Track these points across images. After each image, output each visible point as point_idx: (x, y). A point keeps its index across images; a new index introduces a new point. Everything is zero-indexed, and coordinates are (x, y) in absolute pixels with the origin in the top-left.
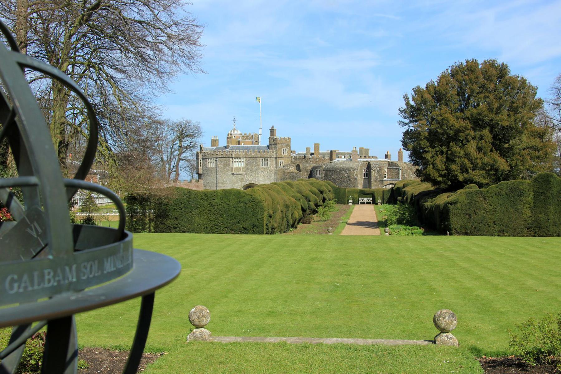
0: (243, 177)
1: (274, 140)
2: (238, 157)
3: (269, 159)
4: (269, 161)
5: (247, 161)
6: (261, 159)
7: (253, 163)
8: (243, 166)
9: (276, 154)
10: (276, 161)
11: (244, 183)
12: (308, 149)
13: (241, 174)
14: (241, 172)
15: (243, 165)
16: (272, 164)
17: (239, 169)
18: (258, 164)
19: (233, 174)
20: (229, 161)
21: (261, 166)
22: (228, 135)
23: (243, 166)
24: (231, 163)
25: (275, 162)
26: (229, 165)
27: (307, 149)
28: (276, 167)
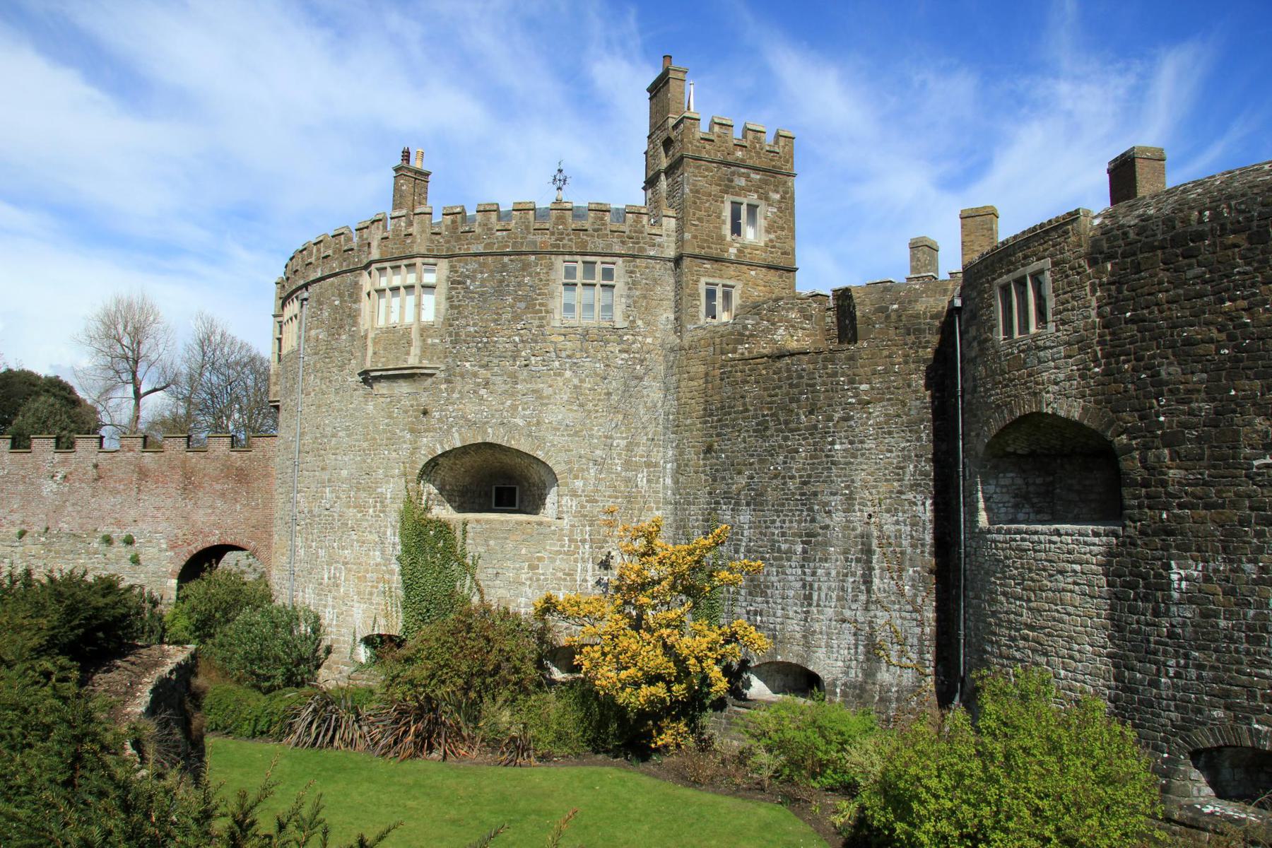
0: (424, 399)
1: (668, 143)
2: (399, 258)
3: (619, 266)
4: (620, 281)
5: (455, 282)
6: (560, 264)
7: (500, 291)
8: (429, 316)
9: (680, 230)
10: (679, 285)
11: (431, 445)
12: (923, 250)
13: (411, 376)
14: (412, 360)
15: (431, 309)
16: (640, 303)
17: (396, 337)
18: (533, 304)
19: (368, 378)
20: (354, 293)
21: (557, 319)
22: (406, 155)
23: (429, 316)
24: (365, 305)
25: (667, 288)
26: (354, 316)
27: (915, 246)
28: (679, 327)
